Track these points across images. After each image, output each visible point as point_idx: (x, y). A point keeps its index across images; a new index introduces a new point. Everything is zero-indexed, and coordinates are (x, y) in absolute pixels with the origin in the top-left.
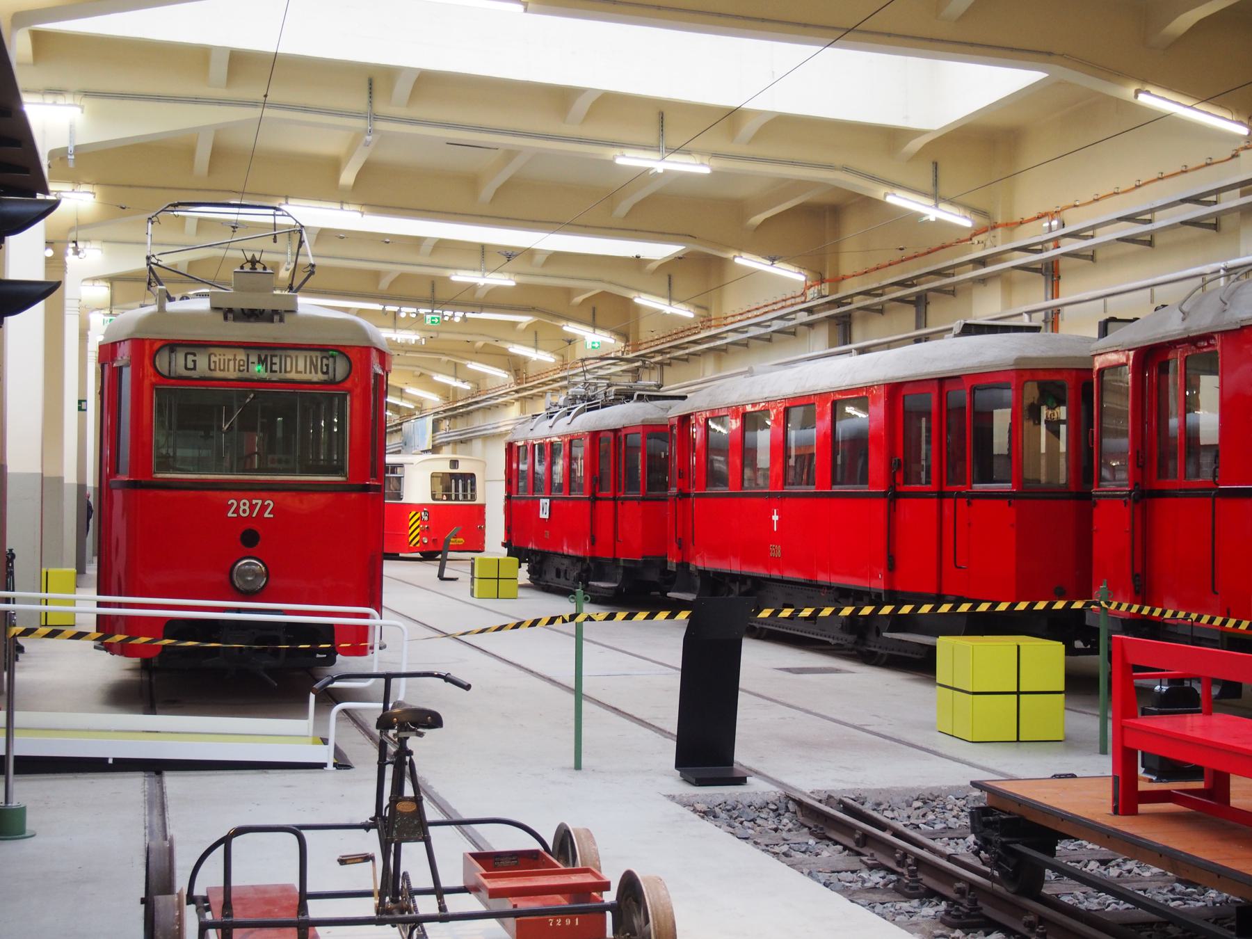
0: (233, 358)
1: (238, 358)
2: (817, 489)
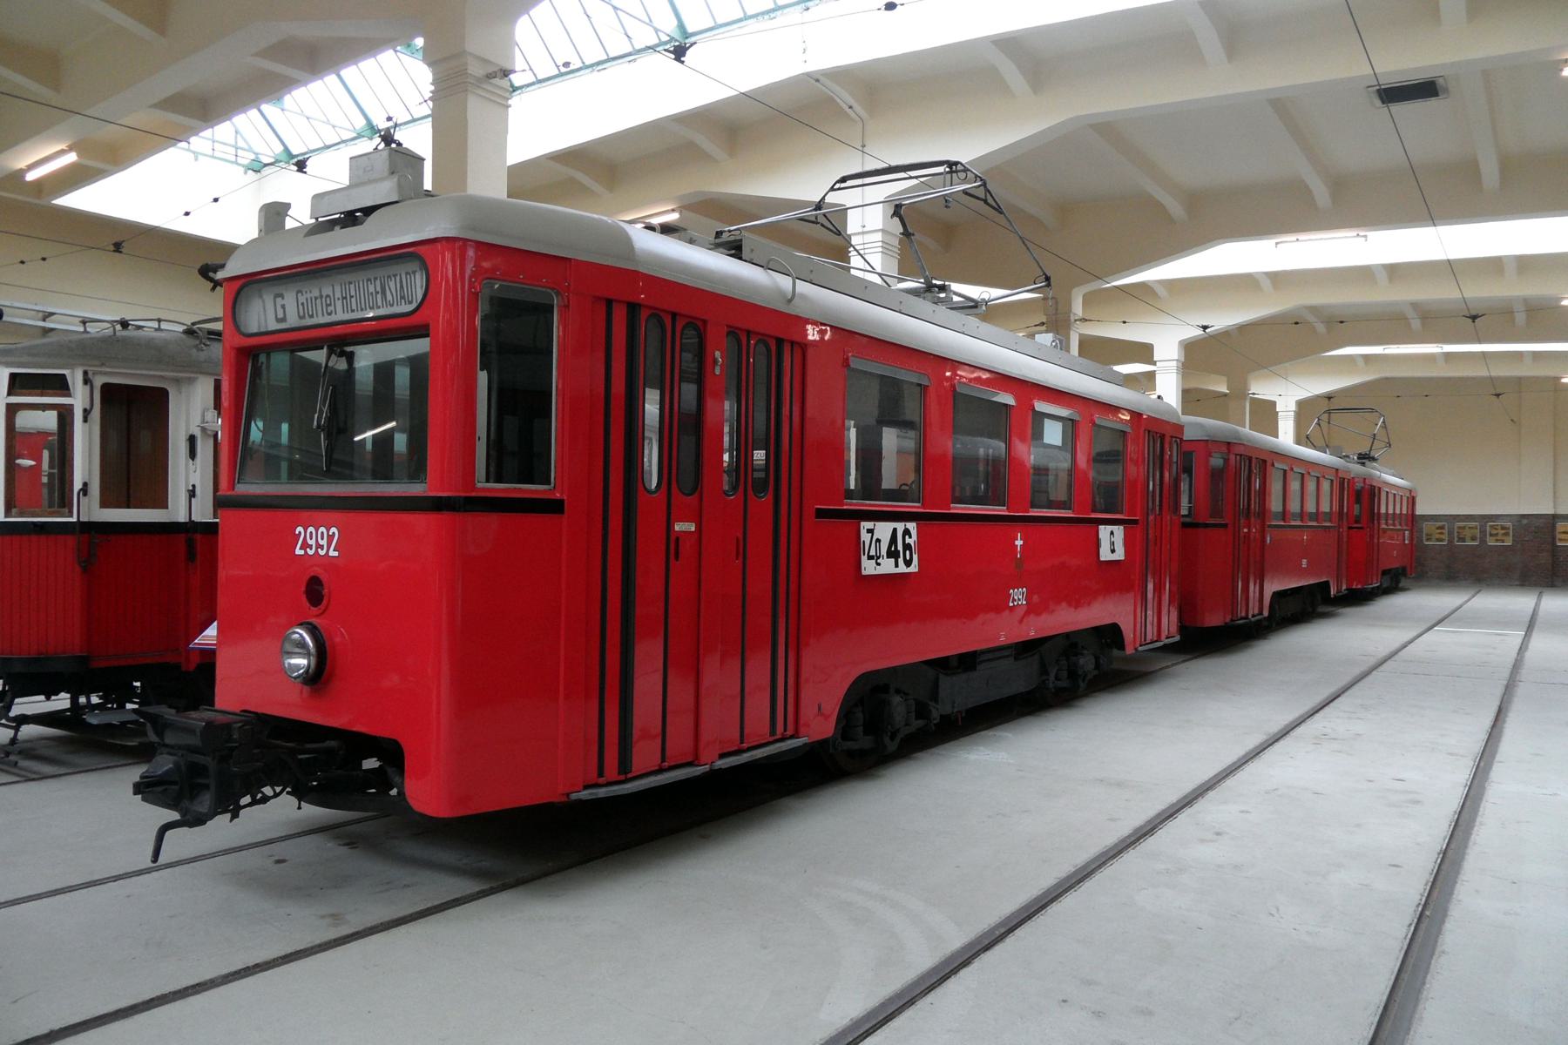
0: (317, 294)
1: (324, 294)
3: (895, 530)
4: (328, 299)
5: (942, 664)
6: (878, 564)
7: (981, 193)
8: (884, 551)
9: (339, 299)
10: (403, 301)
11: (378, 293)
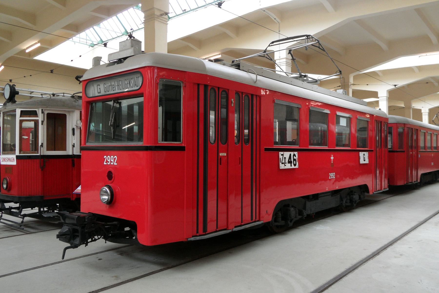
1: (112, 84)
2: (300, 147)
3: (290, 155)
4: (113, 86)
5: (307, 198)
6: (285, 165)
7: (317, 45)
8: (287, 161)
9: (116, 86)
10: (135, 86)
11: (128, 84)
